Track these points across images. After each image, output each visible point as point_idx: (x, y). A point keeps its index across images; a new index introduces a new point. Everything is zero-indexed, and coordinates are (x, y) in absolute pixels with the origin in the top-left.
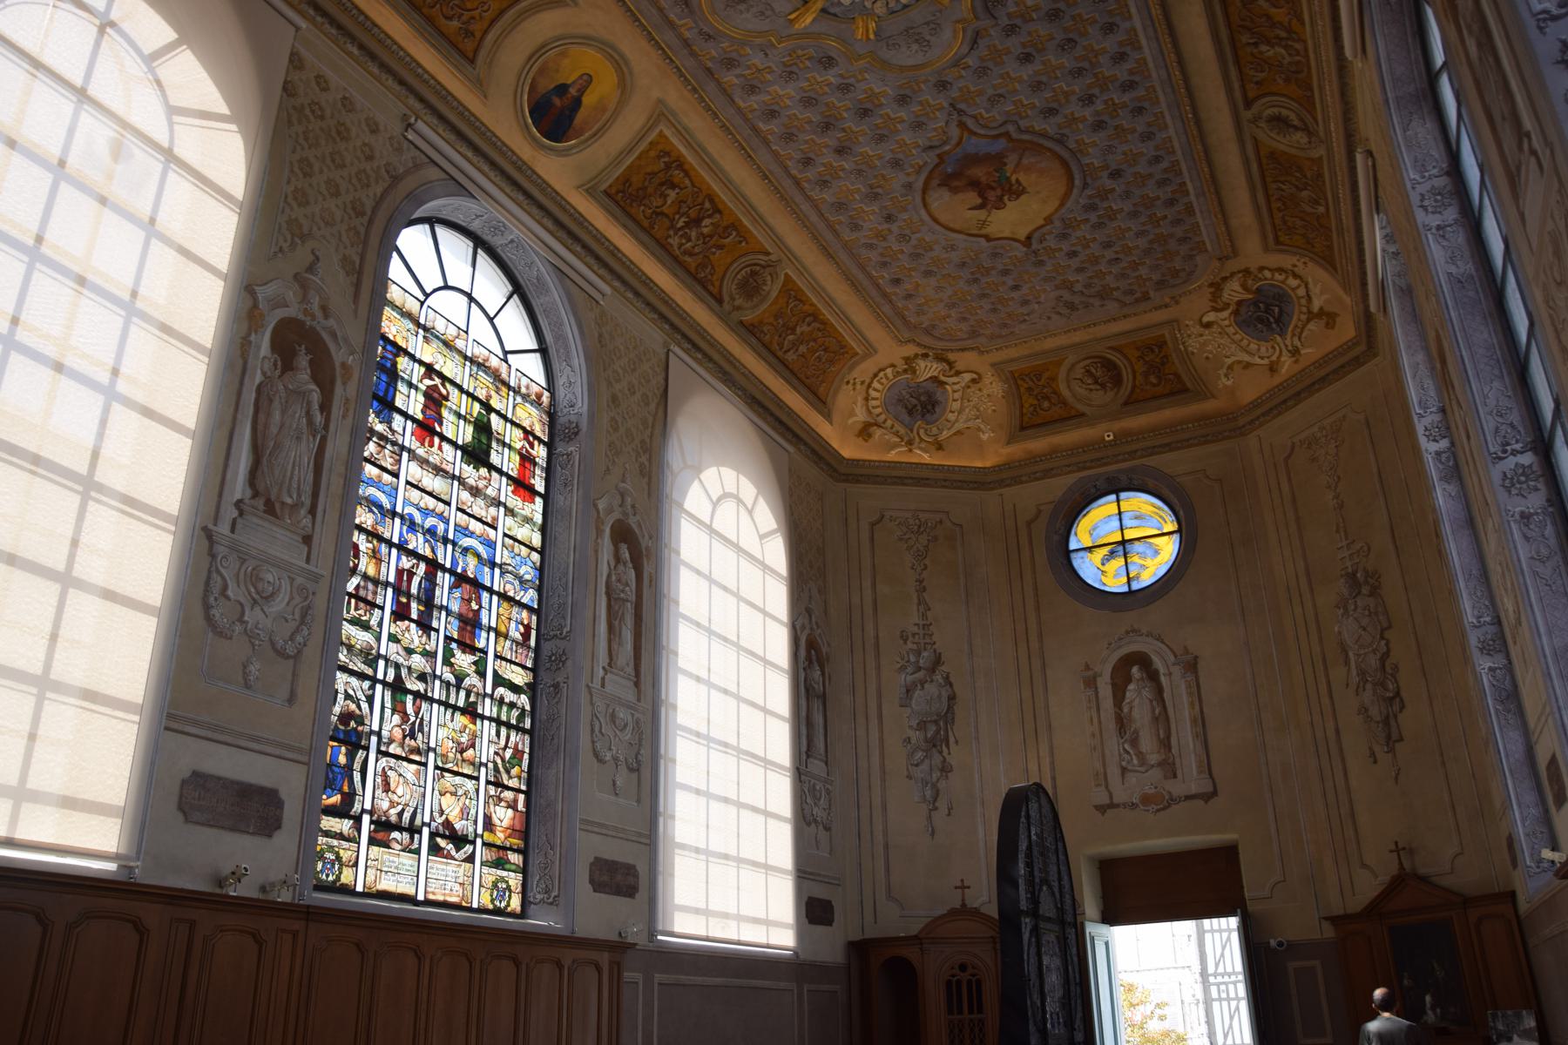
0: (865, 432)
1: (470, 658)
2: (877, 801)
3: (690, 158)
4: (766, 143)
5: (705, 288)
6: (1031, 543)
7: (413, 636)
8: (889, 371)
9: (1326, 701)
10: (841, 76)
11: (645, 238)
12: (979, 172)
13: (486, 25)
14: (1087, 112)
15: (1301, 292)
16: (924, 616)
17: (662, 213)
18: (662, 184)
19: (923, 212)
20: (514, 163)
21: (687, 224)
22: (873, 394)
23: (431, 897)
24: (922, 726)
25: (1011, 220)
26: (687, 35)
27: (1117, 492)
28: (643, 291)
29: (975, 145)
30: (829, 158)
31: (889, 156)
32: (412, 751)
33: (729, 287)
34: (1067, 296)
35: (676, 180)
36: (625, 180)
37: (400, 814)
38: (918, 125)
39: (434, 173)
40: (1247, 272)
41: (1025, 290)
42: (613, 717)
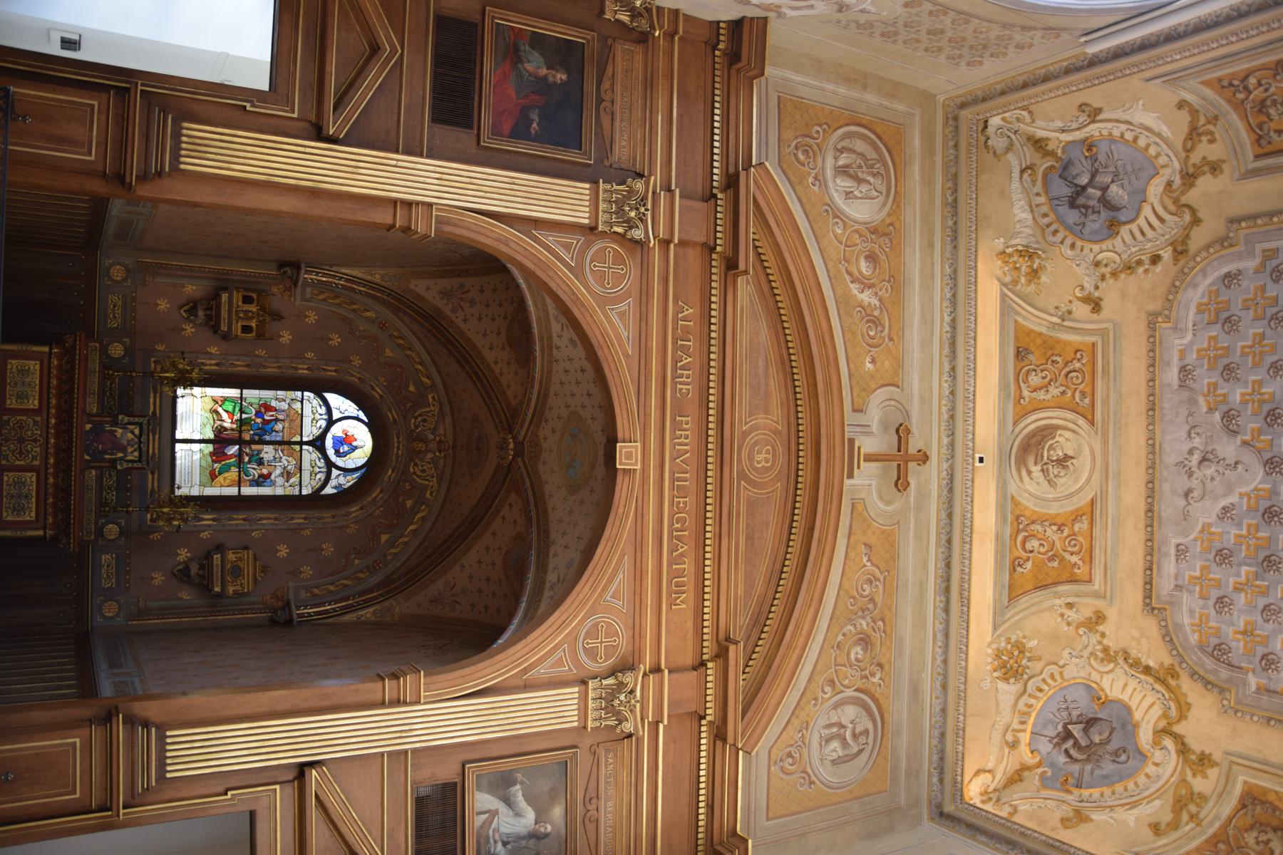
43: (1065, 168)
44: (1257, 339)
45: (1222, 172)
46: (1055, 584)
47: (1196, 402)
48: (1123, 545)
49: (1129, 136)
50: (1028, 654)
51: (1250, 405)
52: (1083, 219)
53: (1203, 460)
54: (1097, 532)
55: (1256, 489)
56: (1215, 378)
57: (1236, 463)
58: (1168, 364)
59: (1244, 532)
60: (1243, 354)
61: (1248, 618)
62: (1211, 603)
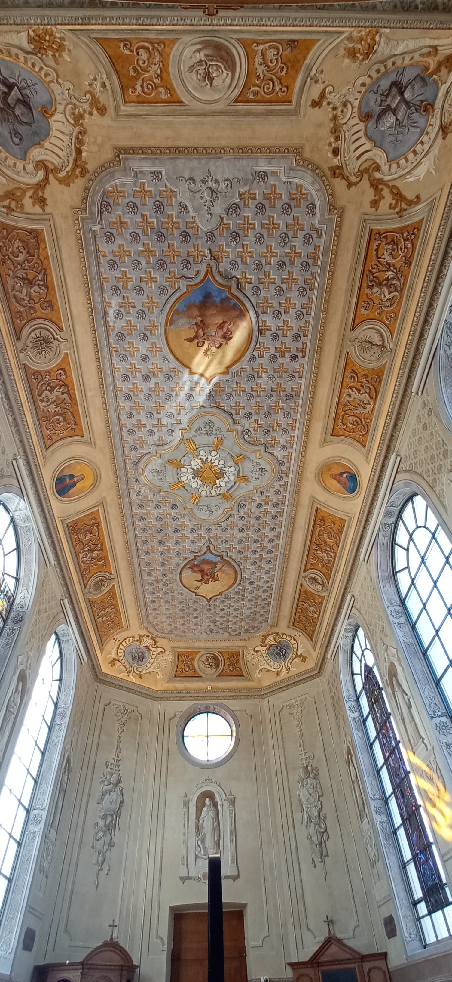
0: (112, 663)
2: (74, 861)
3: (103, 524)
4: (135, 529)
6: (169, 728)
8: (131, 639)
9: (291, 829)
10: (176, 514)
12: (206, 567)
14: (252, 557)
15: (295, 646)
16: (118, 755)
19: (178, 576)
20: (44, 495)
22: (121, 647)
24: (105, 817)
25: (208, 589)
26: (130, 476)
27: (207, 713)
28: (64, 570)
29: (209, 557)
30: (155, 543)
31: (177, 550)
33: (91, 583)
34: (212, 625)
35: (93, 531)
36: (75, 523)
38: (193, 542)
40: (278, 633)
41: (198, 619)
43: (423, 79)
44: (276, 226)
45: (372, 207)
46: (117, 73)
47: (245, 185)
48: (156, 128)
49: (419, 148)
50: (57, 54)
51: (242, 222)
52: (381, 92)
53: (213, 191)
54: (161, 107)
55: (198, 227)
56: (259, 198)
57: (211, 214)
58: (270, 163)
59: (175, 220)
60: (270, 217)
61: (129, 224)
62: (132, 199)
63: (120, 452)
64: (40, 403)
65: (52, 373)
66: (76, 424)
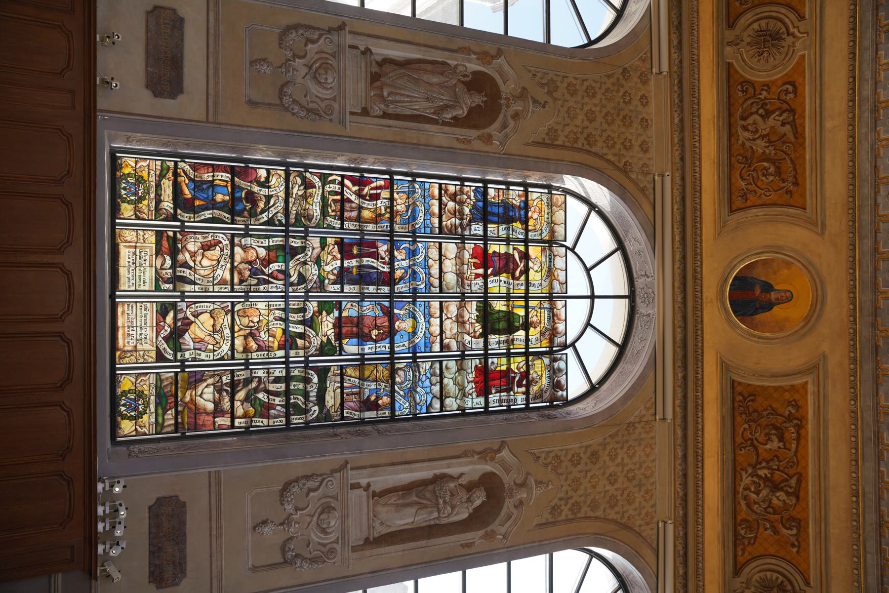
1: (331, 332)
5: (735, 545)
7: (332, 266)
11: (729, 448)
13: (759, 202)
17: (756, 448)
18: (776, 428)
20: (695, 271)
21: (766, 479)
23: (120, 310)
32: (240, 273)
35: (787, 436)
36: (753, 393)
37: (185, 265)
39: (648, 209)
42: (327, 509)
63: (868, 244)
64: (740, 130)
65: (773, 89)
66: (796, 184)
